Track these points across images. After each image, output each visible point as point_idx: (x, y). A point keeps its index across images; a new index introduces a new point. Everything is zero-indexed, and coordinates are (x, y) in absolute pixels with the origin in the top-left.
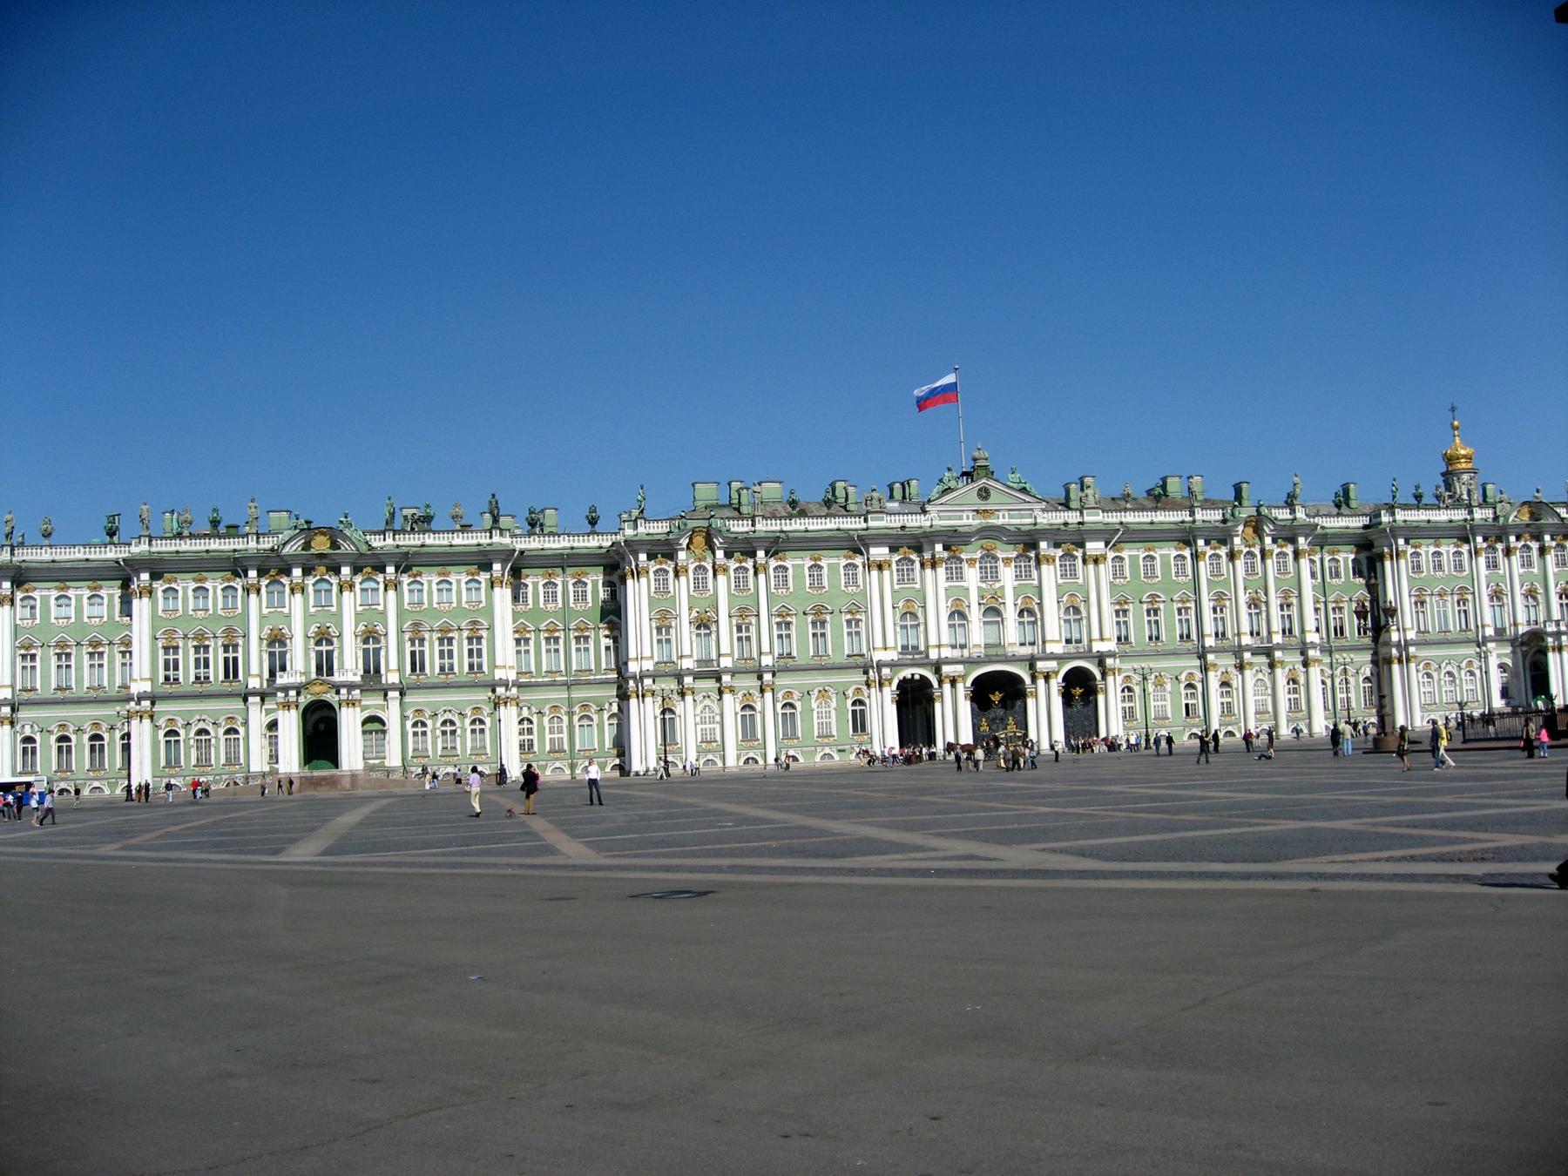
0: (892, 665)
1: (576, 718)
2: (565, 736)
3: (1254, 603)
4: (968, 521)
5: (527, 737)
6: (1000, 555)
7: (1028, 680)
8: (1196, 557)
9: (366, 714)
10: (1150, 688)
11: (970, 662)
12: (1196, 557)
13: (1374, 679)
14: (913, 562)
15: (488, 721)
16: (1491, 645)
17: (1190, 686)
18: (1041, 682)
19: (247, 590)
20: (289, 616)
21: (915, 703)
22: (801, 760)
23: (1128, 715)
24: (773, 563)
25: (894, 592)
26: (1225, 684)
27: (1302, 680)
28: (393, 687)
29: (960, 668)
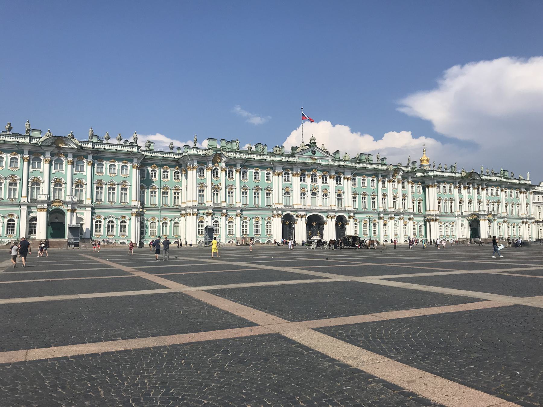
0: (283, 210)
2: (157, 229)
3: (395, 198)
6: (318, 173)
7: (325, 219)
11: (307, 211)
13: (423, 226)
16: (460, 218)
17: (374, 224)
18: (330, 219)
24: (243, 170)
26: (385, 225)
27: (408, 225)
29: (304, 213)
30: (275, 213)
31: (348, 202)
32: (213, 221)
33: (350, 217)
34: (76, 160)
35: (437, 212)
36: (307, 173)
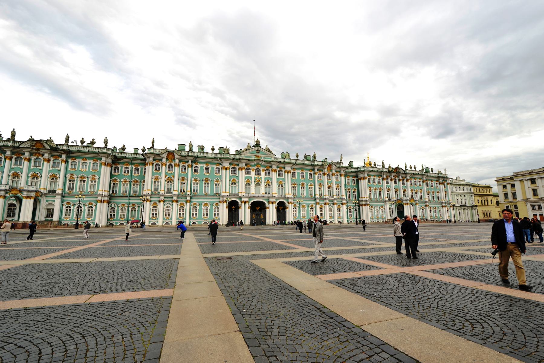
0: (227, 197)
1: (130, 208)
2: (126, 213)
4: (253, 158)
5: (113, 213)
6: (261, 168)
7: (267, 204)
8: (315, 174)
9: (48, 203)
10: (301, 208)
11: (250, 198)
12: (315, 174)
14: (236, 168)
15: (94, 207)
16: (387, 203)
17: (312, 208)
18: (271, 204)
19: (5, 159)
20: (22, 169)
21: (233, 207)
22: (197, 224)
23: (295, 215)
24: (194, 165)
25: (230, 176)
26: (321, 208)
27: (341, 209)
28: (59, 194)
30: (221, 199)
31: (289, 190)
32: (166, 206)
33: (289, 203)
34: (52, 159)
35: (368, 199)
36: (251, 168)
